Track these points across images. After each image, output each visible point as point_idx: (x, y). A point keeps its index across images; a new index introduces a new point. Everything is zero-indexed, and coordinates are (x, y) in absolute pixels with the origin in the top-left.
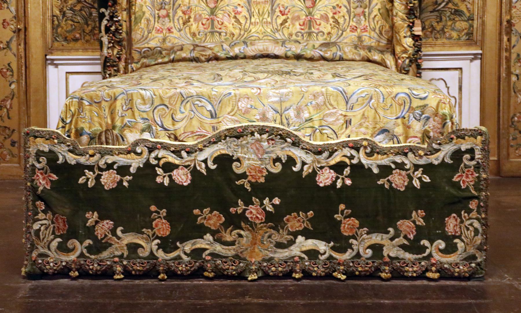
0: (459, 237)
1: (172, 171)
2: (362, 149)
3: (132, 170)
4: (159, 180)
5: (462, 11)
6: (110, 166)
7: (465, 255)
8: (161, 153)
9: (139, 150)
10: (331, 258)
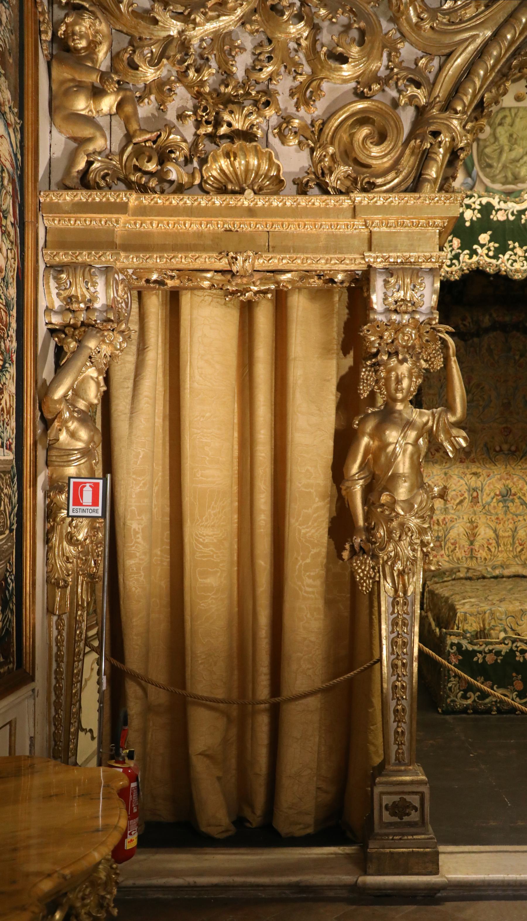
1: (525, 653)
3: (503, 653)
4: (517, 659)
6: (490, 651)
8: (519, 644)
9: (506, 642)
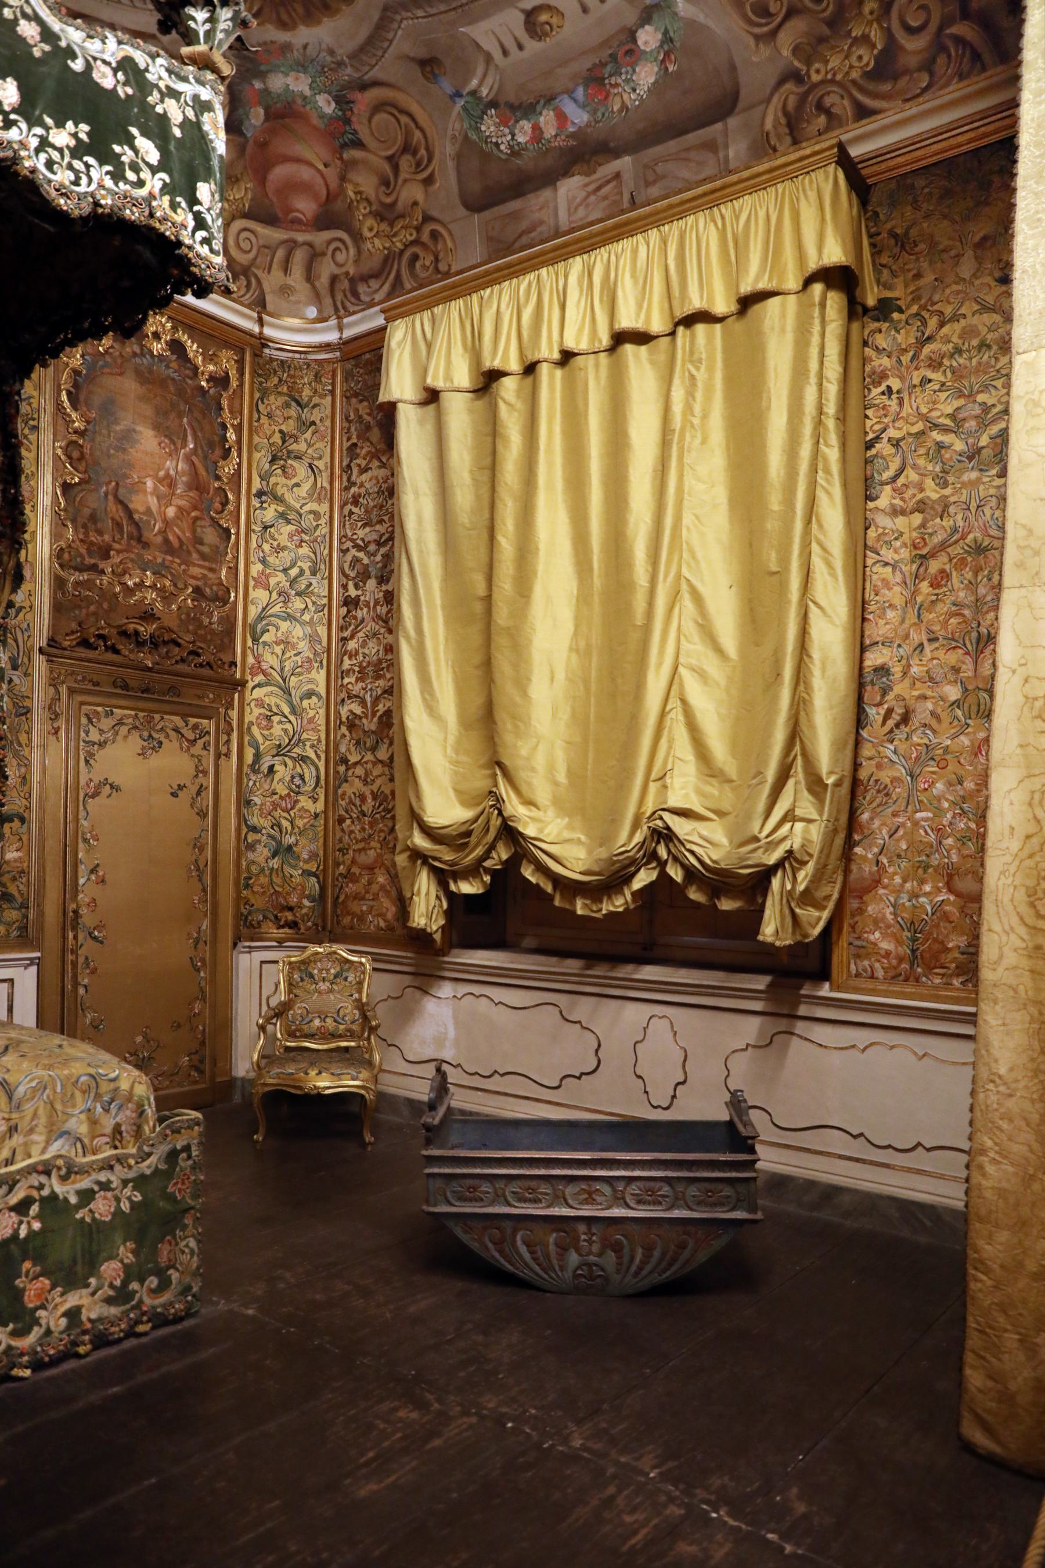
0: (173, 1267)
2: (54, 1172)
5: (12, 895)
7: (180, 1288)
10: (10, 1348)
